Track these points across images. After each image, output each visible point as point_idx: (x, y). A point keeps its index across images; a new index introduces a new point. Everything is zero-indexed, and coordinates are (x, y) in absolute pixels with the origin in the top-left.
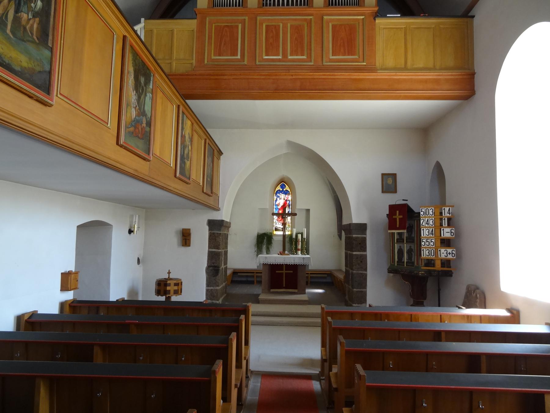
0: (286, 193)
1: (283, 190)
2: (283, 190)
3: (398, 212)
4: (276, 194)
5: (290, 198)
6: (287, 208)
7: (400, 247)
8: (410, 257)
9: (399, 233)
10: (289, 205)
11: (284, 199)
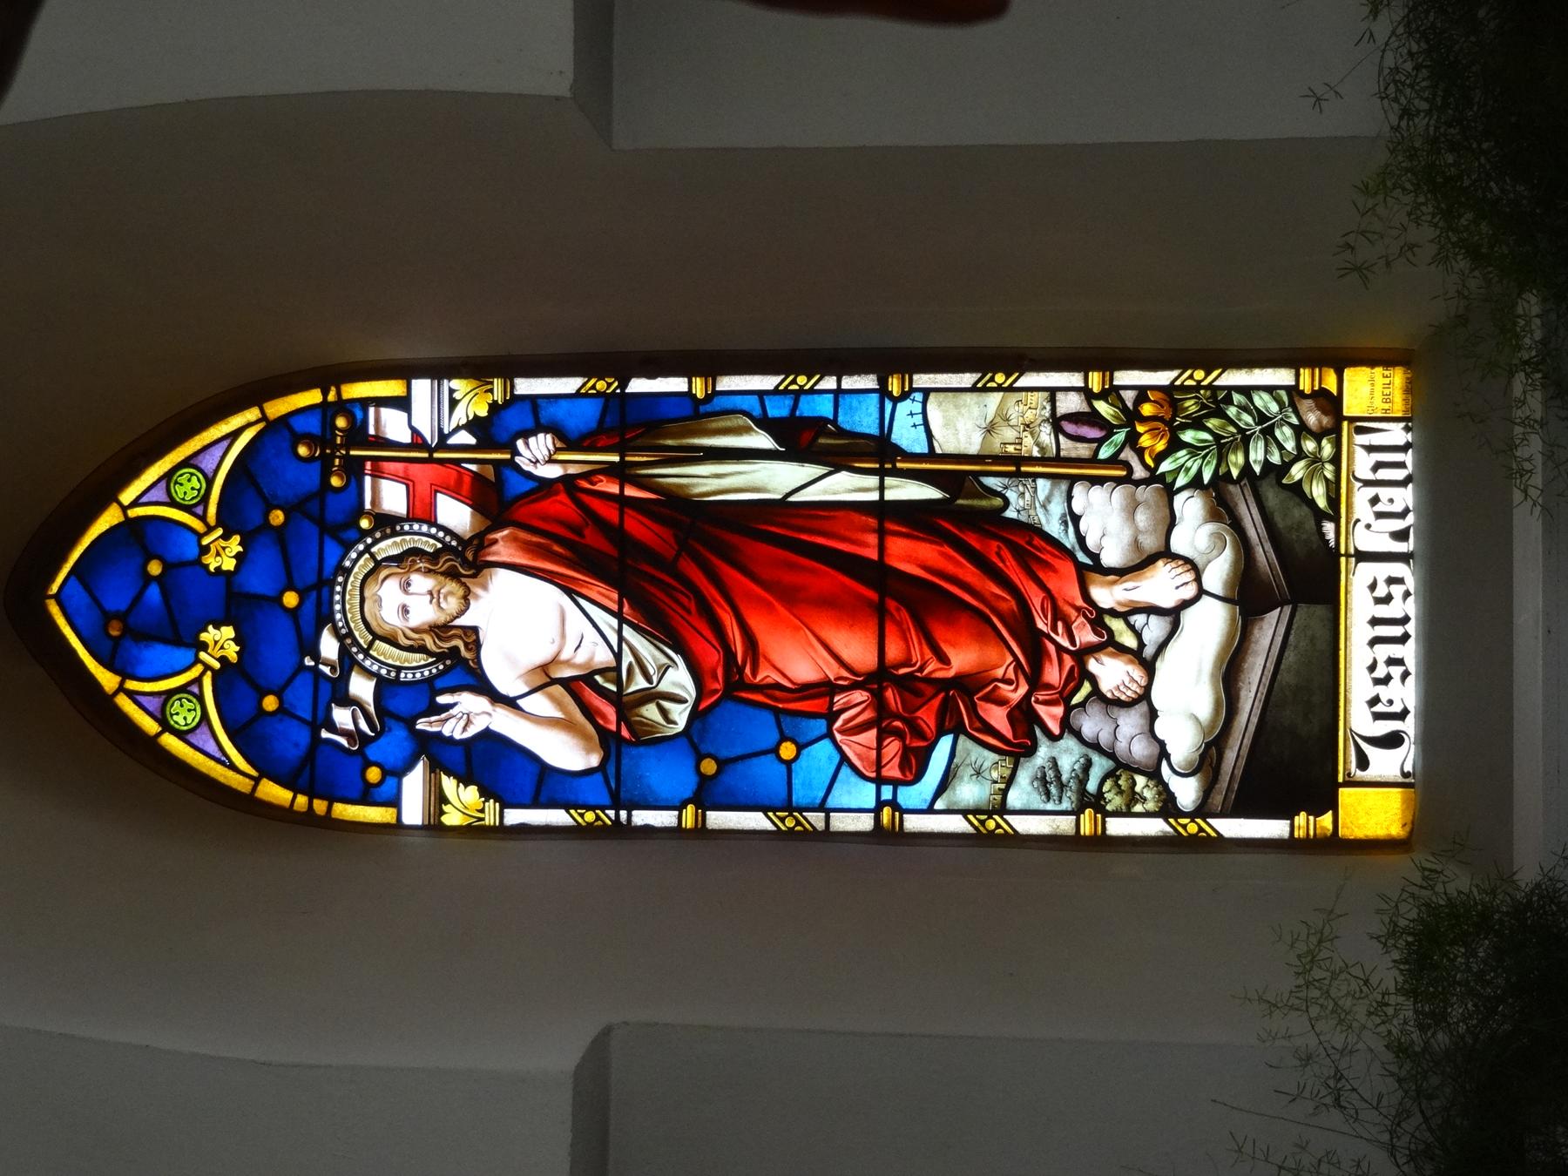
0: (306, 512)
1: (234, 601)
2: (234, 601)
4: (322, 770)
5: (427, 411)
6: (708, 481)
10: (628, 427)
11: (463, 563)
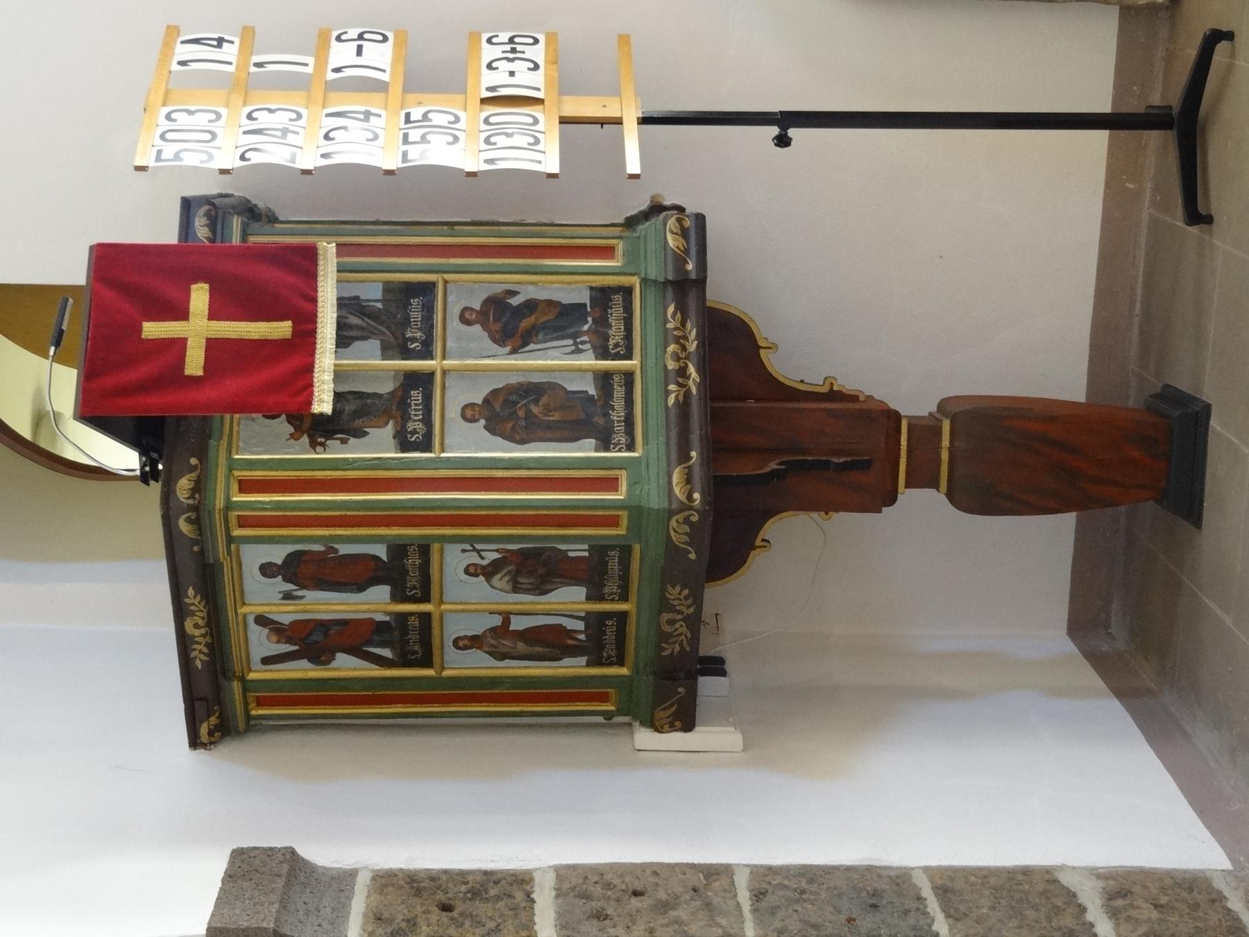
3: (153, 330)
7: (469, 413)
8: (560, 321)
9: (343, 341)
